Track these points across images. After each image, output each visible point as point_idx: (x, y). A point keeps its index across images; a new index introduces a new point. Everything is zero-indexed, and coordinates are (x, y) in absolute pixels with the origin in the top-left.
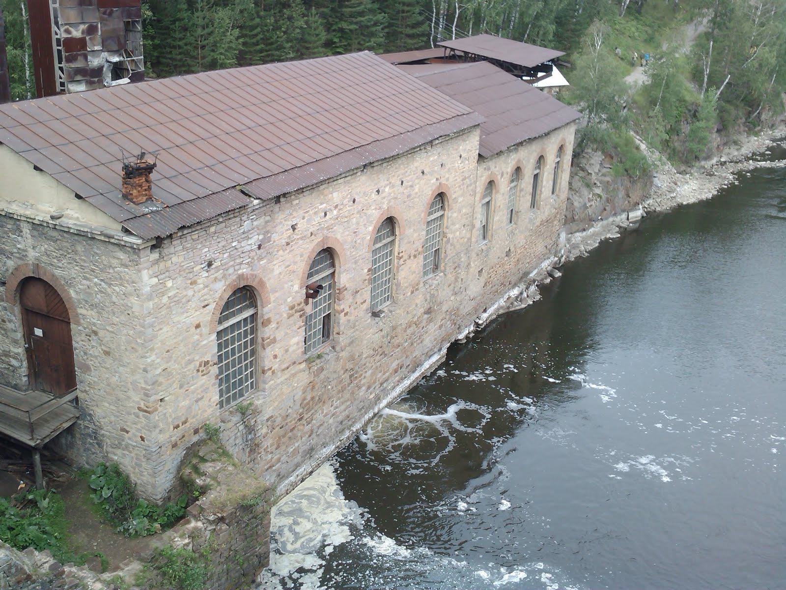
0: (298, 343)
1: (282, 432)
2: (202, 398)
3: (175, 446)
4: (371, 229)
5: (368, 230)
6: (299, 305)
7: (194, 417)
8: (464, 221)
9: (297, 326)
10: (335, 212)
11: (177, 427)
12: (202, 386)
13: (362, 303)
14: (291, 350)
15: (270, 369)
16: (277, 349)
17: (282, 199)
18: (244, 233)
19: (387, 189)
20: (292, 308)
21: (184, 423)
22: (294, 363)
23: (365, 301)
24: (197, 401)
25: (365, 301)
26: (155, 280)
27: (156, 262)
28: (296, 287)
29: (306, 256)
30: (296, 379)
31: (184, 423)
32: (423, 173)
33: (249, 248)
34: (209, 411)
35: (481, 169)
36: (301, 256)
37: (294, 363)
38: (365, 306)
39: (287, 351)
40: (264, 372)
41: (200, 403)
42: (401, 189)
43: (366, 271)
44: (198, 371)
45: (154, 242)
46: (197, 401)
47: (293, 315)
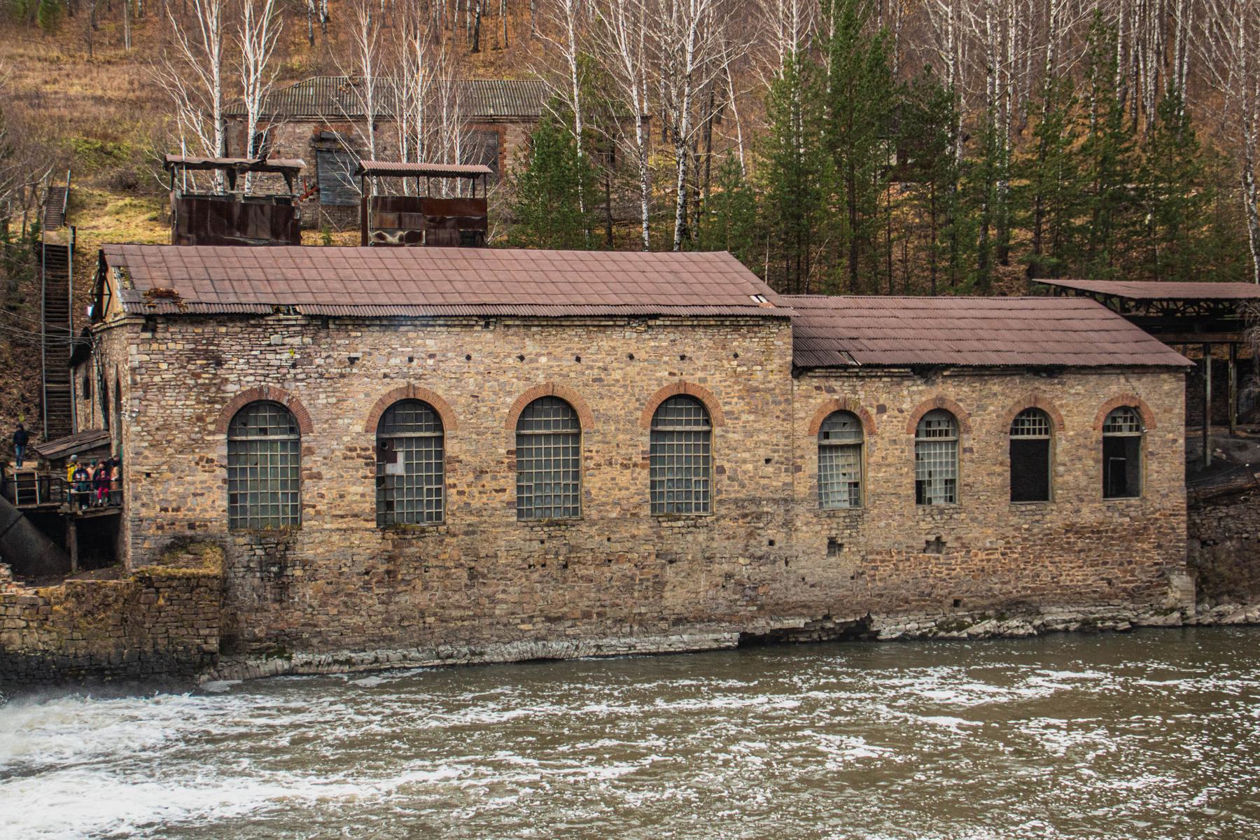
0: (363, 495)
1: (329, 589)
2: (202, 494)
3: (160, 527)
4: (510, 400)
5: (509, 404)
6: (366, 449)
7: (189, 510)
8: (763, 453)
9: (360, 473)
10: (430, 362)
11: (166, 510)
12: (201, 482)
13: (497, 491)
14: (349, 498)
15: (314, 507)
16: (323, 486)
17: (331, 326)
18: (270, 345)
19: (543, 360)
20: (351, 450)
21: (177, 510)
22: (355, 516)
23: (504, 490)
24: (195, 495)
25: (504, 490)
26: (147, 358)
27: (144, 341)
28: (359, 428)
29: (376, 397)
30: (358, 536)
31: (177, 510)
32: (631, 357)
33: (278, 363)
34: (211, 514)
35: (804, 386)
36: (367, 395)
37: (355, 516)
38: (506, 497)
39: (342, 496)
40: (303, 506)
41: (199, 498)
42: (578, 367)
43: (502, 451)
44: (197, 464)
45: (143, 321)
46: (195, 495)
47: (352, 458)
